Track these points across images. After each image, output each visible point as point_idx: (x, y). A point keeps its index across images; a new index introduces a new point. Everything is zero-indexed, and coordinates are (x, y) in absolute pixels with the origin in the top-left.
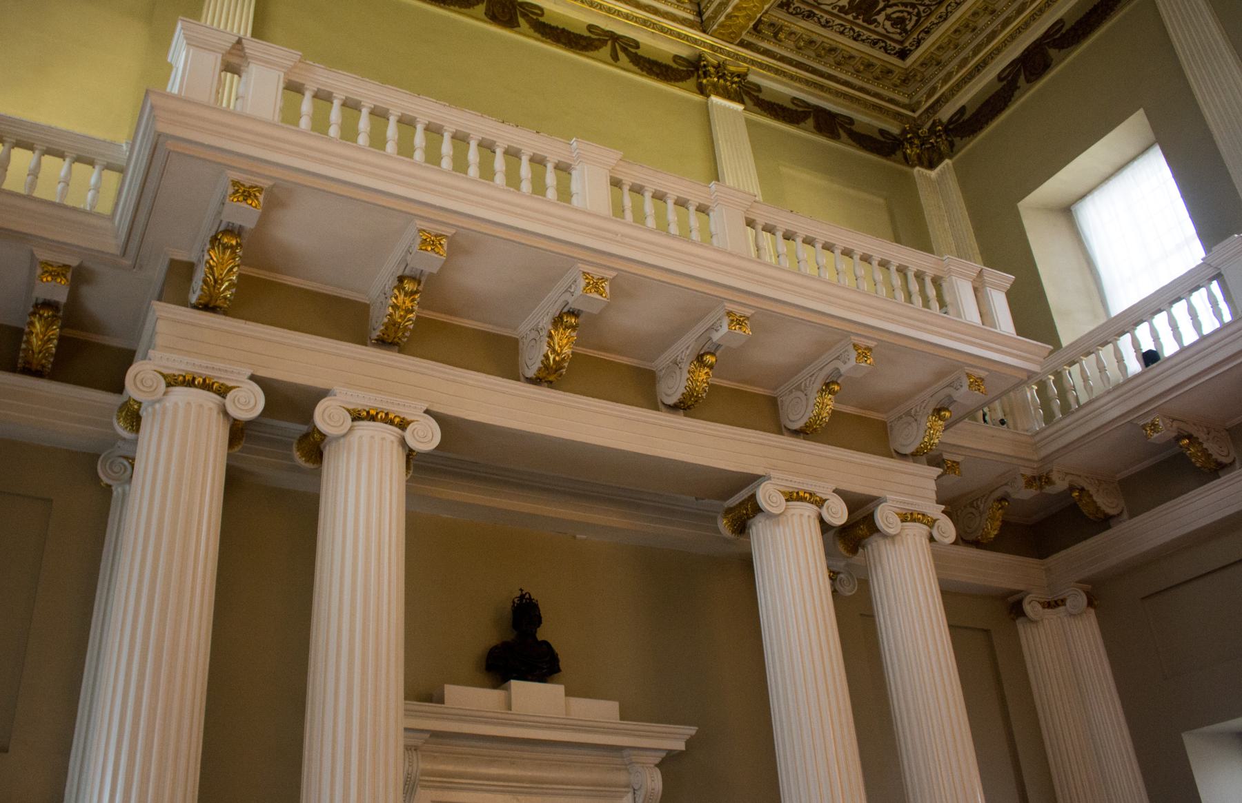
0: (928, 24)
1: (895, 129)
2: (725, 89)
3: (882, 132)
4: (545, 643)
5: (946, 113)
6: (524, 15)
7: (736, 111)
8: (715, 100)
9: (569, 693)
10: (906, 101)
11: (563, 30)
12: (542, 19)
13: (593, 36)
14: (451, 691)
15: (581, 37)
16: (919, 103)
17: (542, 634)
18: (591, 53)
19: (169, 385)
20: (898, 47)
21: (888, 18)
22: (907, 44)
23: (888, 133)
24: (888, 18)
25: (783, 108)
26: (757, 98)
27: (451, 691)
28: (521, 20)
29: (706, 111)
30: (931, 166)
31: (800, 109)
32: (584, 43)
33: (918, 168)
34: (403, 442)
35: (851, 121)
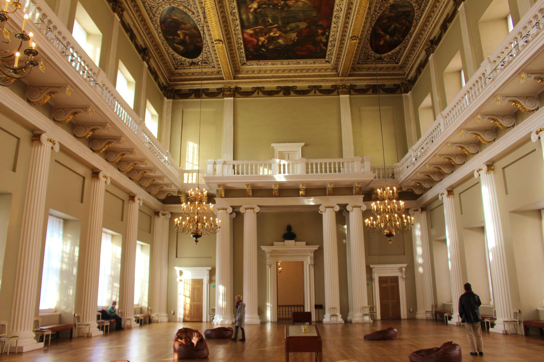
0: (398, 57)
1: (398, 82)
2: (344, 91)
3: (395, 85)
4: (293, 233)
5: (409, 78)
6: (292, 90)
7: (347, 97)
8: (341, 96)
9: (295, 241)
10: (403, 72)
11: (302, 90)
12: (296, 89)
13: (310, 89)
14: (275, 243)
15: (307, 90)
16: (406, 73)
17: (292, 231)
18: (309, 94)
19: (219, 210)
20: (394, 62)
21: (387, 59)
22: (396, 61)
23: (396, 84)
24: (387, 59)
25: (362, 90)
26: (355, 89)
27: (275, 243)
28: (292, 92)
29: (339, 98)
30: (408, 92)
31: (368, 88)
32: (307, 92)
33: (403, 94)
34: (254, 211)
35: (384, 85)
